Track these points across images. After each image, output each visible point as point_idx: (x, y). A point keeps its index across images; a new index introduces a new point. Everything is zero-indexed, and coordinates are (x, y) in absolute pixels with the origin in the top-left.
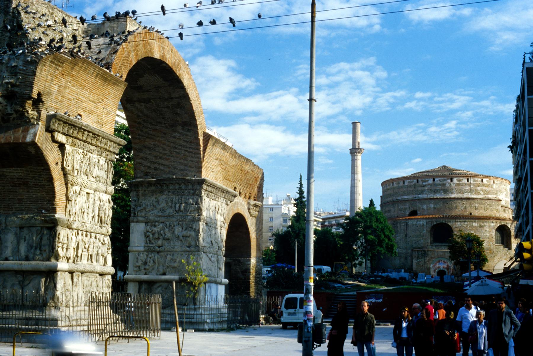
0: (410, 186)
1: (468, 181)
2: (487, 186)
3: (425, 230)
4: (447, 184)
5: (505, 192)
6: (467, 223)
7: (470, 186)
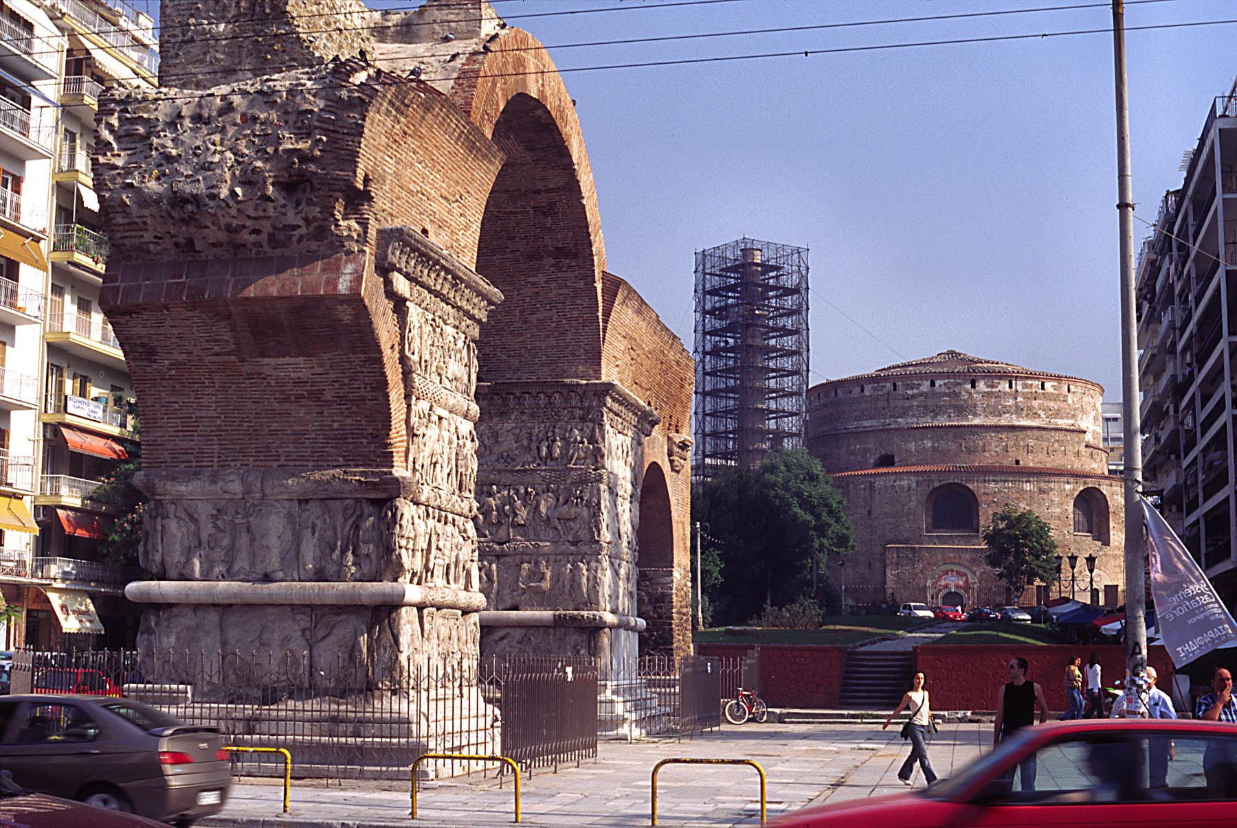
0: (877, 398)
1: (1011, 387)
2: (1054, 398)
4: (963, 393)
5: (1093, 413)
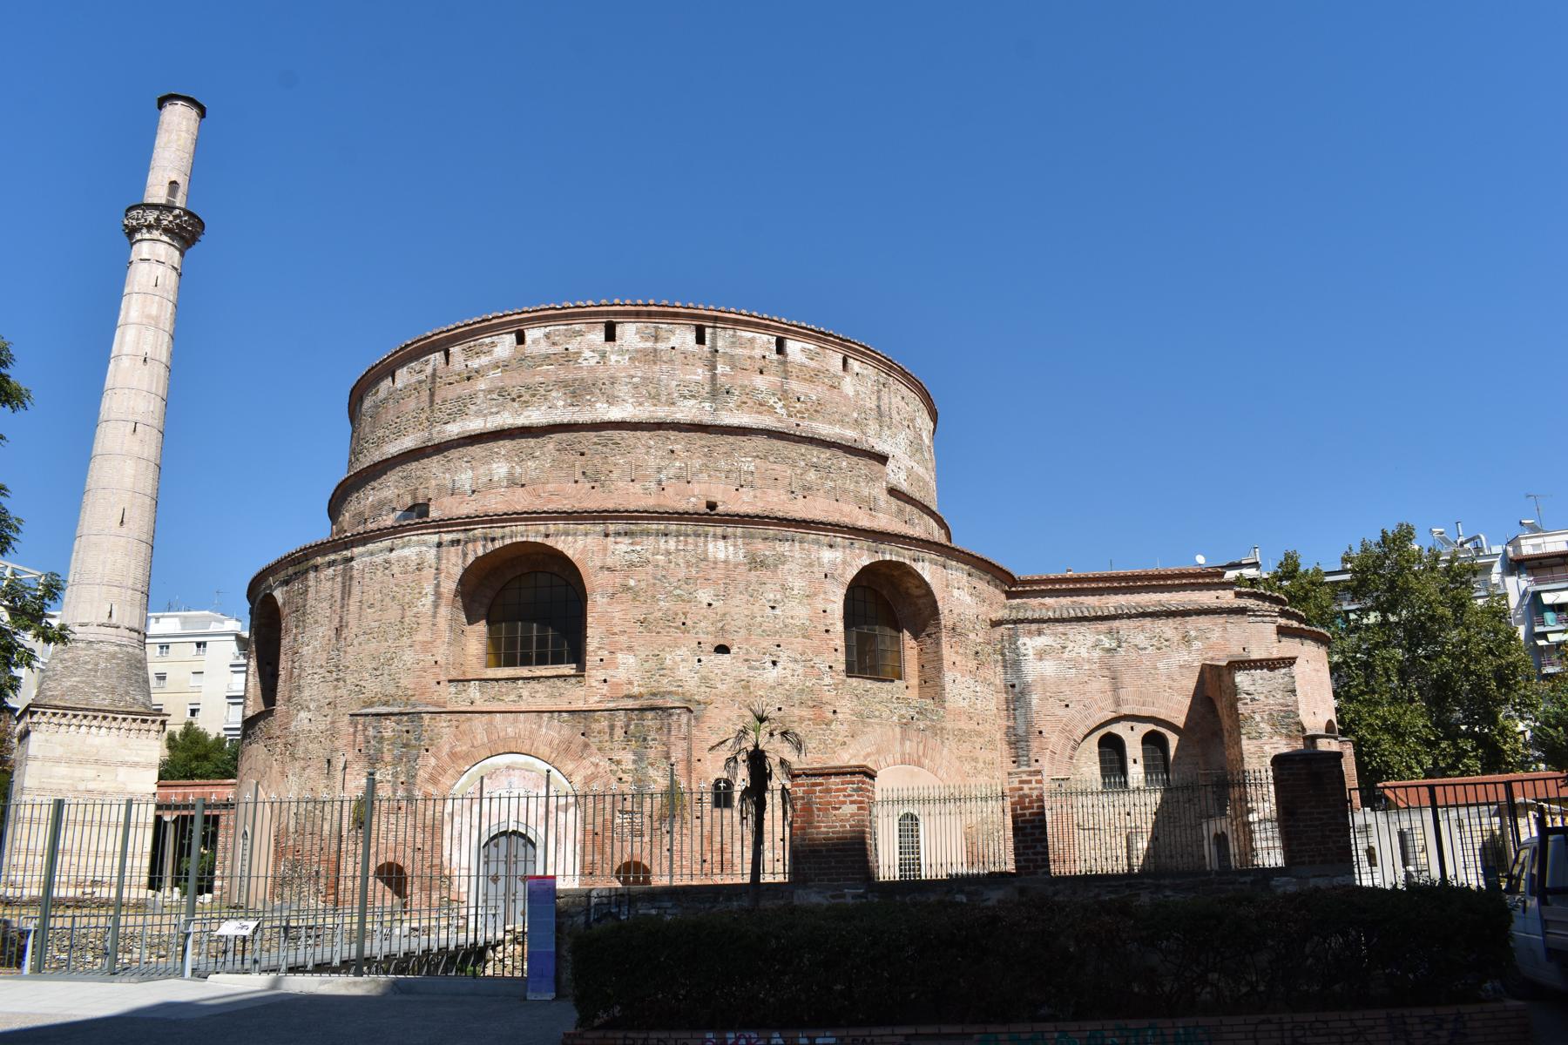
1: (700, 340)
3: (429, 588)
4: (587, 354)
6: (672, 544)
7: (715, 368)
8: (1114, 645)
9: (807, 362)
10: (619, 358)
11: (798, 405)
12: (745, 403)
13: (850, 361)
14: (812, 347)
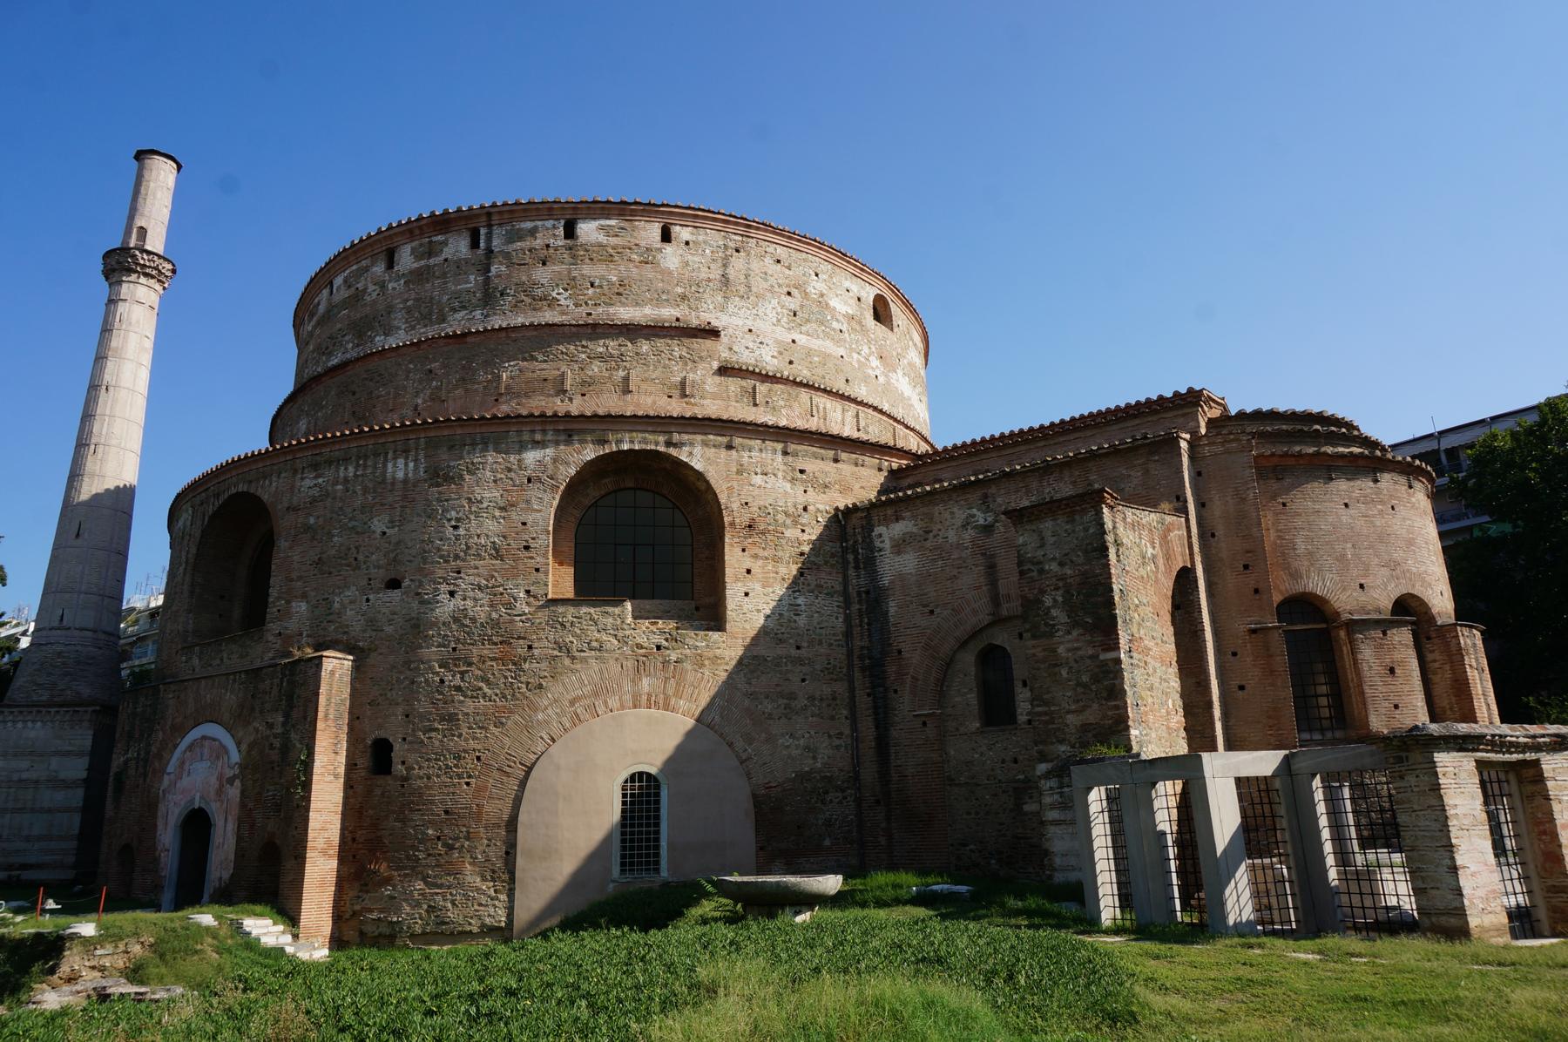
1: (475, 244)
2: (607, 256)
4: (371, 288)
7: (489, 271)
8: (990, 519)
9: (602, 238)
10: (395, 285)
11: (591, 291)
12: (523, 301)
13: (676, 230)
14: (613, 222)
